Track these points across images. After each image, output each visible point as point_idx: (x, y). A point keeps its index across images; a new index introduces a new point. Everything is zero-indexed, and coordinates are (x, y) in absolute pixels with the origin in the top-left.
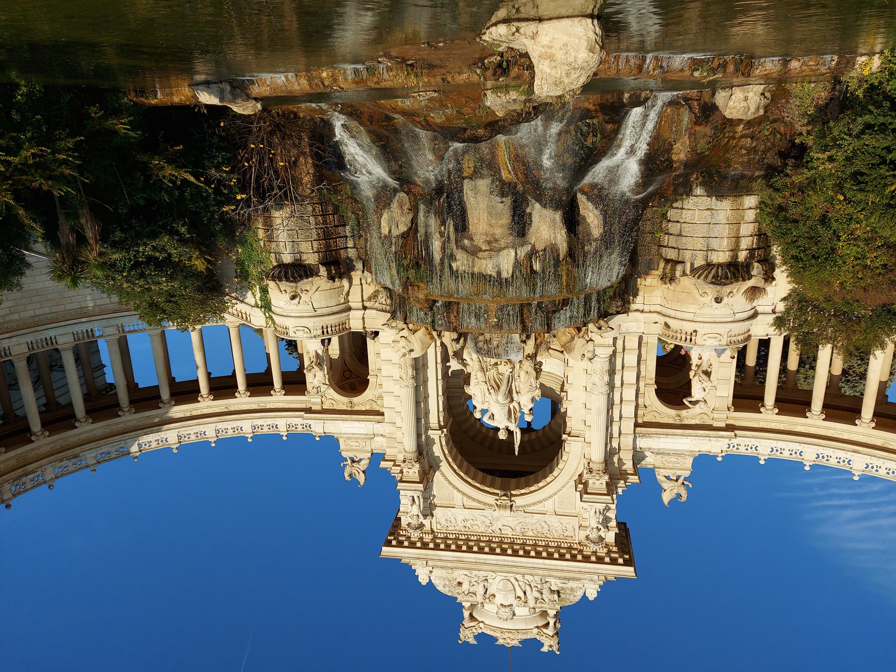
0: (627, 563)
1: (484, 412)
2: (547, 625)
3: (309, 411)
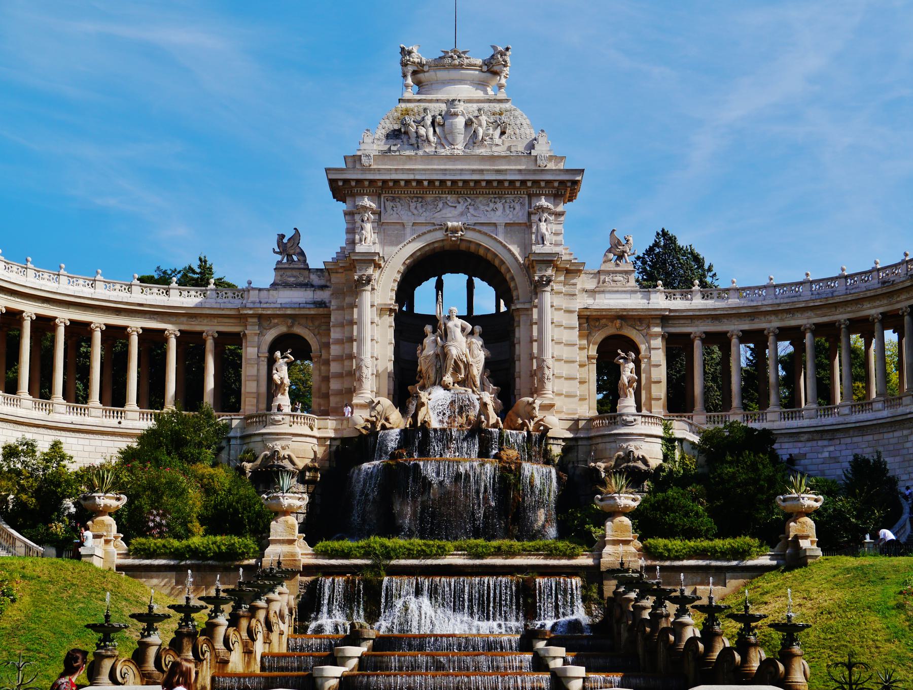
0: (336, 181)
1: (472, 333)
2: (414, 73)
3: (664, 318)
